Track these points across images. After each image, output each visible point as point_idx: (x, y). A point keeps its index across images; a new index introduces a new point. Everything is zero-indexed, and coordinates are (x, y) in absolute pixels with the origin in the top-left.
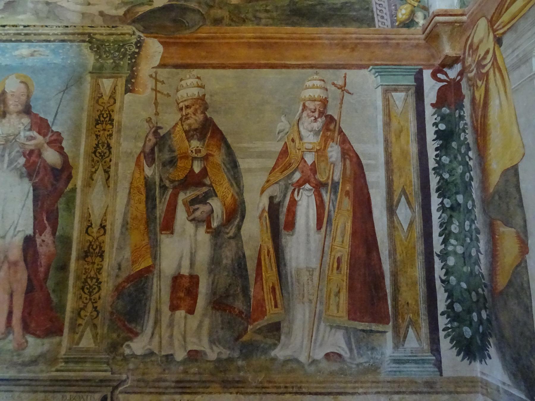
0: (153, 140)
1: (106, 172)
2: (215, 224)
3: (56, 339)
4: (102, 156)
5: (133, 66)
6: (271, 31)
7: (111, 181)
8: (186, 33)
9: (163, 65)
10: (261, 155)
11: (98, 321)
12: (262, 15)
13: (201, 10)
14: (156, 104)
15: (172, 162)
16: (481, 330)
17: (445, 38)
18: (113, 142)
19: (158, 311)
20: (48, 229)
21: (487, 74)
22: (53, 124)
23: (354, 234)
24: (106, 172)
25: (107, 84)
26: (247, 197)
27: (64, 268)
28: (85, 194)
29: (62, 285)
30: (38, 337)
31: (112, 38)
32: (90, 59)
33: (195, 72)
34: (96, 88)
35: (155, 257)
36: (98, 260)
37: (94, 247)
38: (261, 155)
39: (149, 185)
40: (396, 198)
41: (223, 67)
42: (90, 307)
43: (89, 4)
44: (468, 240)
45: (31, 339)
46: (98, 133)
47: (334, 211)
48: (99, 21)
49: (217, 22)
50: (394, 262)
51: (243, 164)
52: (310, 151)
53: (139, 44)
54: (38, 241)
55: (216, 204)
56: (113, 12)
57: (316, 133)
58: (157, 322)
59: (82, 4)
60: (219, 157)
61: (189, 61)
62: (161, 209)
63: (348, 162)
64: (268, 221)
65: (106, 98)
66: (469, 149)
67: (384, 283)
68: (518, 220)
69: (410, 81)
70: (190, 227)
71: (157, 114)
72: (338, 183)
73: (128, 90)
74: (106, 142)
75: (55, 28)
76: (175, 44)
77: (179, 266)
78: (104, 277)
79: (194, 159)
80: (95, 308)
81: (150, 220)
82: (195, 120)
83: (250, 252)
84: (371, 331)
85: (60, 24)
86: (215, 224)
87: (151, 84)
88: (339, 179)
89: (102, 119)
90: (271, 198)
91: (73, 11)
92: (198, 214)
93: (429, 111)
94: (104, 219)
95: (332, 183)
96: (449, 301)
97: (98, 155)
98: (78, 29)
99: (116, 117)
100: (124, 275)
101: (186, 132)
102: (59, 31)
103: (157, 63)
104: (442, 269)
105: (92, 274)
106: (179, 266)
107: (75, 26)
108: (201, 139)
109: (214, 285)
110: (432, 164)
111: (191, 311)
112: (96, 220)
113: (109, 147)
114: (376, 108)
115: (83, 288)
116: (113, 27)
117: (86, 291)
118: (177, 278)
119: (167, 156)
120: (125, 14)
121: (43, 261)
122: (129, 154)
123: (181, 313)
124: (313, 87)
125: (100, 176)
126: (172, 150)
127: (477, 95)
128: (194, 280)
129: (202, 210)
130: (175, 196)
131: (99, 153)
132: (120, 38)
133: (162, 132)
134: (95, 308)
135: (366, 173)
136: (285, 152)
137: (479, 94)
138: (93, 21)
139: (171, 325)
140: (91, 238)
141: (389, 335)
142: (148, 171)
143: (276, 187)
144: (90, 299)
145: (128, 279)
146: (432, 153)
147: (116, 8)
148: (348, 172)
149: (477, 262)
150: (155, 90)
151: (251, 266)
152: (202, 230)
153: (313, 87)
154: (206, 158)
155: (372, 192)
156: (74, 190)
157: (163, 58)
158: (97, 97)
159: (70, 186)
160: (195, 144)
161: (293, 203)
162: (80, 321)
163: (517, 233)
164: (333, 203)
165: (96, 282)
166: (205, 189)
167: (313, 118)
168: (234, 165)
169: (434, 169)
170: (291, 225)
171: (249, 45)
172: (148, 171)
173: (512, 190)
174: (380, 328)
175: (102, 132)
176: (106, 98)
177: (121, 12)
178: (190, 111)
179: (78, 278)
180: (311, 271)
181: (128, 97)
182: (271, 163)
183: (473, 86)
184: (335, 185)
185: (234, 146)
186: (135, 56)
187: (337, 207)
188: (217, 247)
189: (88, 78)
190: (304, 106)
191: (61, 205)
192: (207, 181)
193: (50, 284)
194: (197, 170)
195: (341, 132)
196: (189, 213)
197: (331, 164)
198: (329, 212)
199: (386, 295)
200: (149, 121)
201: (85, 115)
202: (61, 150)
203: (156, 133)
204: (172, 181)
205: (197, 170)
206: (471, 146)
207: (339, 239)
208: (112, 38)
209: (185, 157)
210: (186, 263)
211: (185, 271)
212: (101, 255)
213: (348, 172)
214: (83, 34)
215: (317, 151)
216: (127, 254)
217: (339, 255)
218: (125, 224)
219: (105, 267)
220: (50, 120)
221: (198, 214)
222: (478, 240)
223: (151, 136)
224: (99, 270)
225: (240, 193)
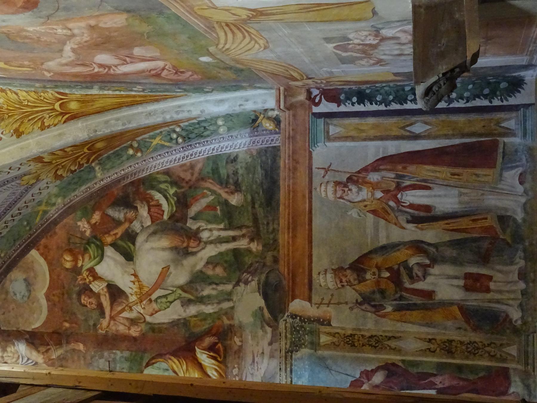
0: (365, 306)
1: (390, 338)
2: (427, 262)
3: (511, 372)
4: (378, 341)
5: (310, 320)
6: (283, 222)
7: (398, 335)
8: (285, 282)
9: (310, 300)
10: (376, 228)
11: (498, 343)
12: (271, 228)
13: (267, 272)
14: (339, 303)
15: (382, 292)
17: (294, 100)
18: (368, 334)
19: (490, 301)
20: (432, 379)
22: (354, 377)
23: (433, 164)
24: (390, 338)
25: (324, 339)
26: (407, 239)
27: (460, 368)
28: (406, 354)
29: (473, 369)
30: (510, 384)
31: (289, 336)
32: (305, 351)
33: (315, 275)
34: (327, 346)
35: (451, 303)
36: (454, 344)
37: (445, 346)
38: (376, 228)
39: (399, 309)
40: (408, 134)
41: (310, 256)
42: (488, 349)
43: (263, 353)
45: (512, 390)
46: (361, 344)
47: (417, 177)
48: (276, 346)
49: (276, 260)
50: (453, 136)
51: (383, 241)
52: (373, 195)
53: (294, 316)
54: (441, 386)
55: (413, 261)
56: (269, 336)
57: (360, 189)
58: (498, 302)
59: (263, 359)
60: (378, 259)
61: (306, 281)
62: (417, 300)
63: (381, 167)
64: (424, 224)
65: (335, 340)
67: (469, 143)
69: (321, 122)
70: (429, 279)
71: (346, 303)
72: (397, 174)
73: (329, 324)
74: (367, 339)
75: (281, 378)
76: (293, 291)
77: (458, 286)
78: (466, 339)
79: (379, 276)
80: (489, 345)
81: (425, 308)
82: (351, 276)
83: (447, 237)
84: (503, 152)
85: (279, 374)
86: (427, 262)
87: (324, 308)
88: (394, 174)
89: (350, 342)
90: (408, 222)
91: (268, 364)
92: (420, 274)
93: (343, 108)
94: (424, 340)
95: (397, 179)
96: (482, 97)
97: (377, 345)
98: (282, 360)
99: (349, 332)
100: (465, 326)
101: (360, 282)
102: (283, 374)
103: (308, 304)
104: (458, 102)
105: (464, 347)
106: (458, 286)
107: (280, 363)
108: (365, 271)
109: (472, 263)
110: (382, 107)
111: (490, 278)
112: (424, 345)
113: (371, 337)
114: (341, 147)
115: (475, 354)
116: (280, 335)
117: (476, 352)
118: (467, 288)
119: (378, 296)
120: (271, 327)
121: (455, 383)
122: (376, 322)
123: (492, 285)
124: (326, 191)
125: (393, 344)
126: (374, 292)
128: (467, 276)
129: (417, 271)
130: (407, 290)
131: (376, 344)
132: (289, 330)
133: (360, 299)
134: (489, 345)
135: (389, 154)
136: (374, 212)
138: (276, 350)
139: (500, 292)
140: (438, 349)
141: (506, 140)
142: (389, 309)
143: (400, 218)
144: (483, 348)
145: (467, 322)
146: (374, 107)
147: (266, 332)
148: (388, 167)
150: (328, 304)
151: (458, 236)
152: (432, 271)
153: (326, 191)
154: (379, 268)
155: (403, 150)
156: (403, 361)
157: (304, 299)
158: (334, 346)
159: (400, 364)
160: (368, 276)
161: (411, 206)
162: (498, 356)
164: (411, 178)
165: (470, 345)
166: (402, 269)
167: (349, 192)
168: (384, 248)
169: (386, 106)
170: (428, 208)
171: (294, 237)
172: (389, 309)
174: (501, 146)
175: (360, 342)
176: (335, 340)
177: (269, 330)
178: (344, 280)
179: (467, 358)
180: (461, 194)
181: (334, 323)
182: (382, 222)
184: (398, 177)
185: (369, 248)
186: (302, 319)
187: (414, 175)
188: (444, 260)
189: (320, 352)
190: (341, 198)
191: (414, 370)
192: (396, 267)
193: (471, 377)
194: (387, 274)
195: (359, 172)
196: (418, 279)
197: (383, 180)
198: (418, 181)
199: (478, 141)
200: (351, 309)
201: (347, 354)
202: (374, 371)
203: (361, 304)
204: (396, 292)
205: (387, 274)
207: (438, 175)
208: (289, 336)
209: (378, 283)
210: (456, 282)
211: (461, 282)
212: (451, 341)
213: (388, 167)
214: (286, 358)
215: (373, 189)
216: (449, 323)
217: (449, 175)
218: (428, 325)
219: (459, 338)
220: (351, 379)
221: (420, 274)
223: (363, 307)
224: (462, 343)
225: (404, 244)
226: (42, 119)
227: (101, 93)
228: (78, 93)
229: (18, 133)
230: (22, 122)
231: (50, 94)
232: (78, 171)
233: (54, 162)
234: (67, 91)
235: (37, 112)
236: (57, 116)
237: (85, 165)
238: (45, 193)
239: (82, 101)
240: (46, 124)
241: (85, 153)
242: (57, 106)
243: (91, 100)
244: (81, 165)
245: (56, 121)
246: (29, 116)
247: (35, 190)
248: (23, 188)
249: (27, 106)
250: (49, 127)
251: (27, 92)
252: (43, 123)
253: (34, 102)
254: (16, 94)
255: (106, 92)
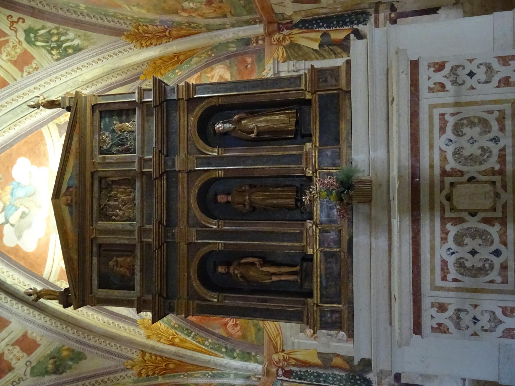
16: (362, 380)
17: (270, 369)
21: (289, 357)
44: (335, 379)
66: (307, 371)
68: (331, 355)
69: (280, 382)
110: (310, 382)
127: (293, 363)
137: (293, 362)
146: (306, 382)
149: (342, 376)
163: (335, 357)
173: (324, 355)
183: (289, 365)
206: (307, 369)
222: (335, 374)
226: (161, 338)
227: (191, 341)
228: (183, 336)
229: (148, 337)
230: (153, 335)
231: (173, 331)
232: (150, 376)
233: (147, 362)
234: (179, 333)
235: (162, 335)
236: (167, 341)
237: (156, 375)
238: (127, 379)
239: (181, 340)
240: (161, 341)
241: (162, 366)
242: (170, 337)
243: (186, 341)
244: (154, 374)
245: (166, 342)
246: (157, 334)
247: (123, 374)
248: (123, 367)
249: (160, 331)
250: (161, 342)
251: (165, 326)
252: (160, 340)
253: (164, 331)
254: (161, 325)
255: (193, 341)
